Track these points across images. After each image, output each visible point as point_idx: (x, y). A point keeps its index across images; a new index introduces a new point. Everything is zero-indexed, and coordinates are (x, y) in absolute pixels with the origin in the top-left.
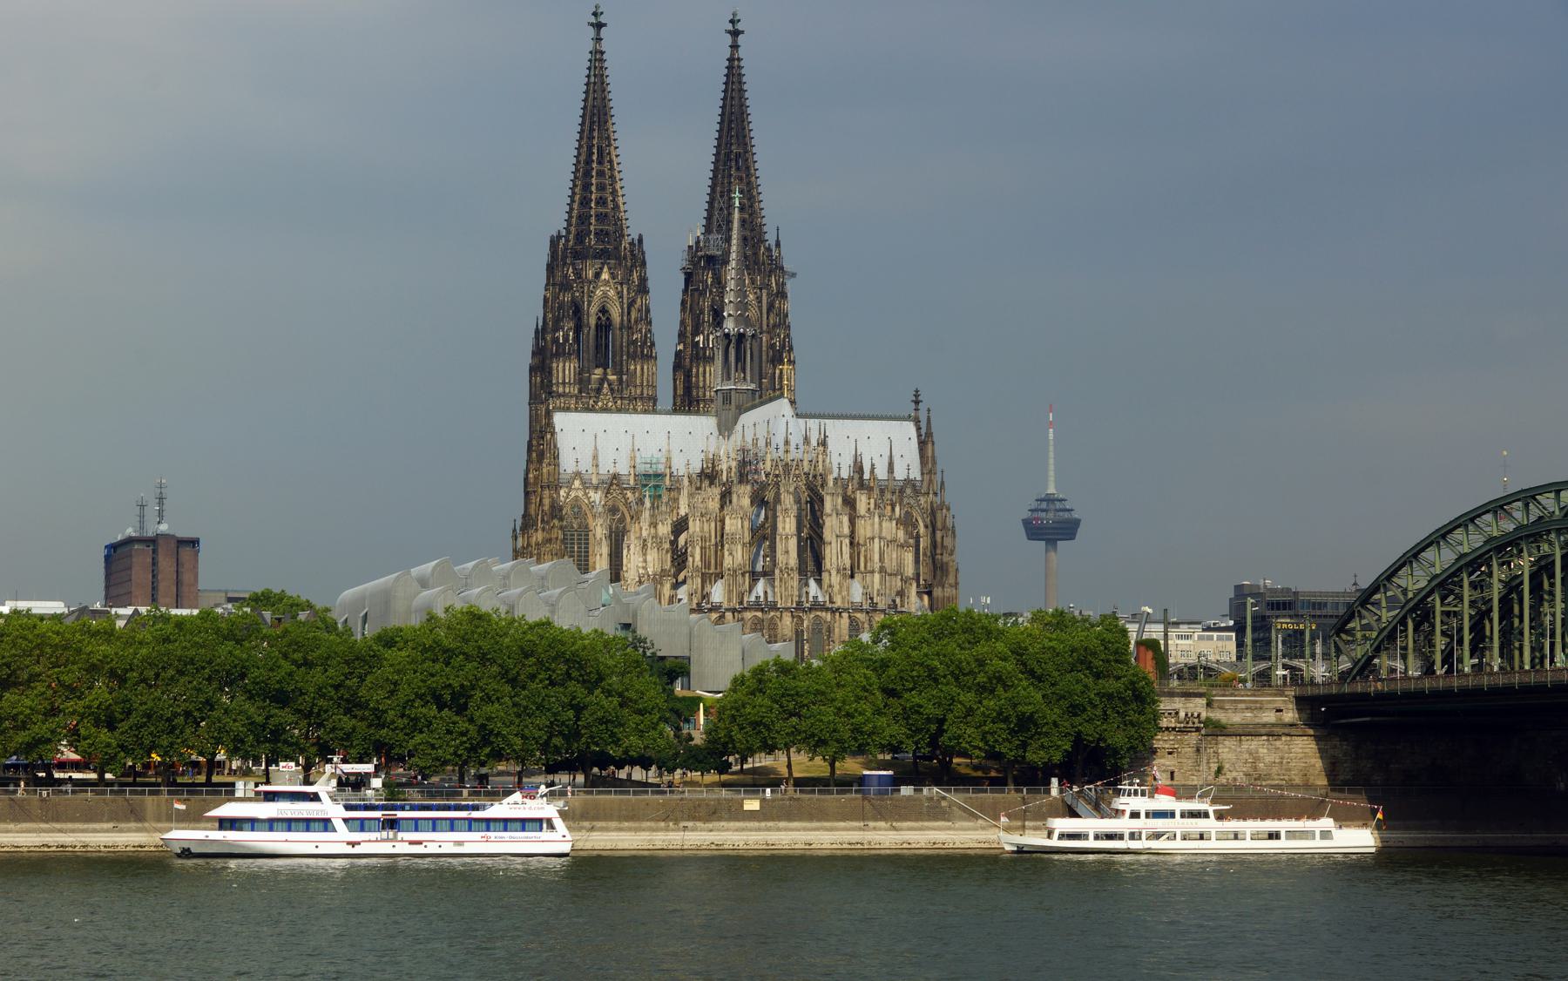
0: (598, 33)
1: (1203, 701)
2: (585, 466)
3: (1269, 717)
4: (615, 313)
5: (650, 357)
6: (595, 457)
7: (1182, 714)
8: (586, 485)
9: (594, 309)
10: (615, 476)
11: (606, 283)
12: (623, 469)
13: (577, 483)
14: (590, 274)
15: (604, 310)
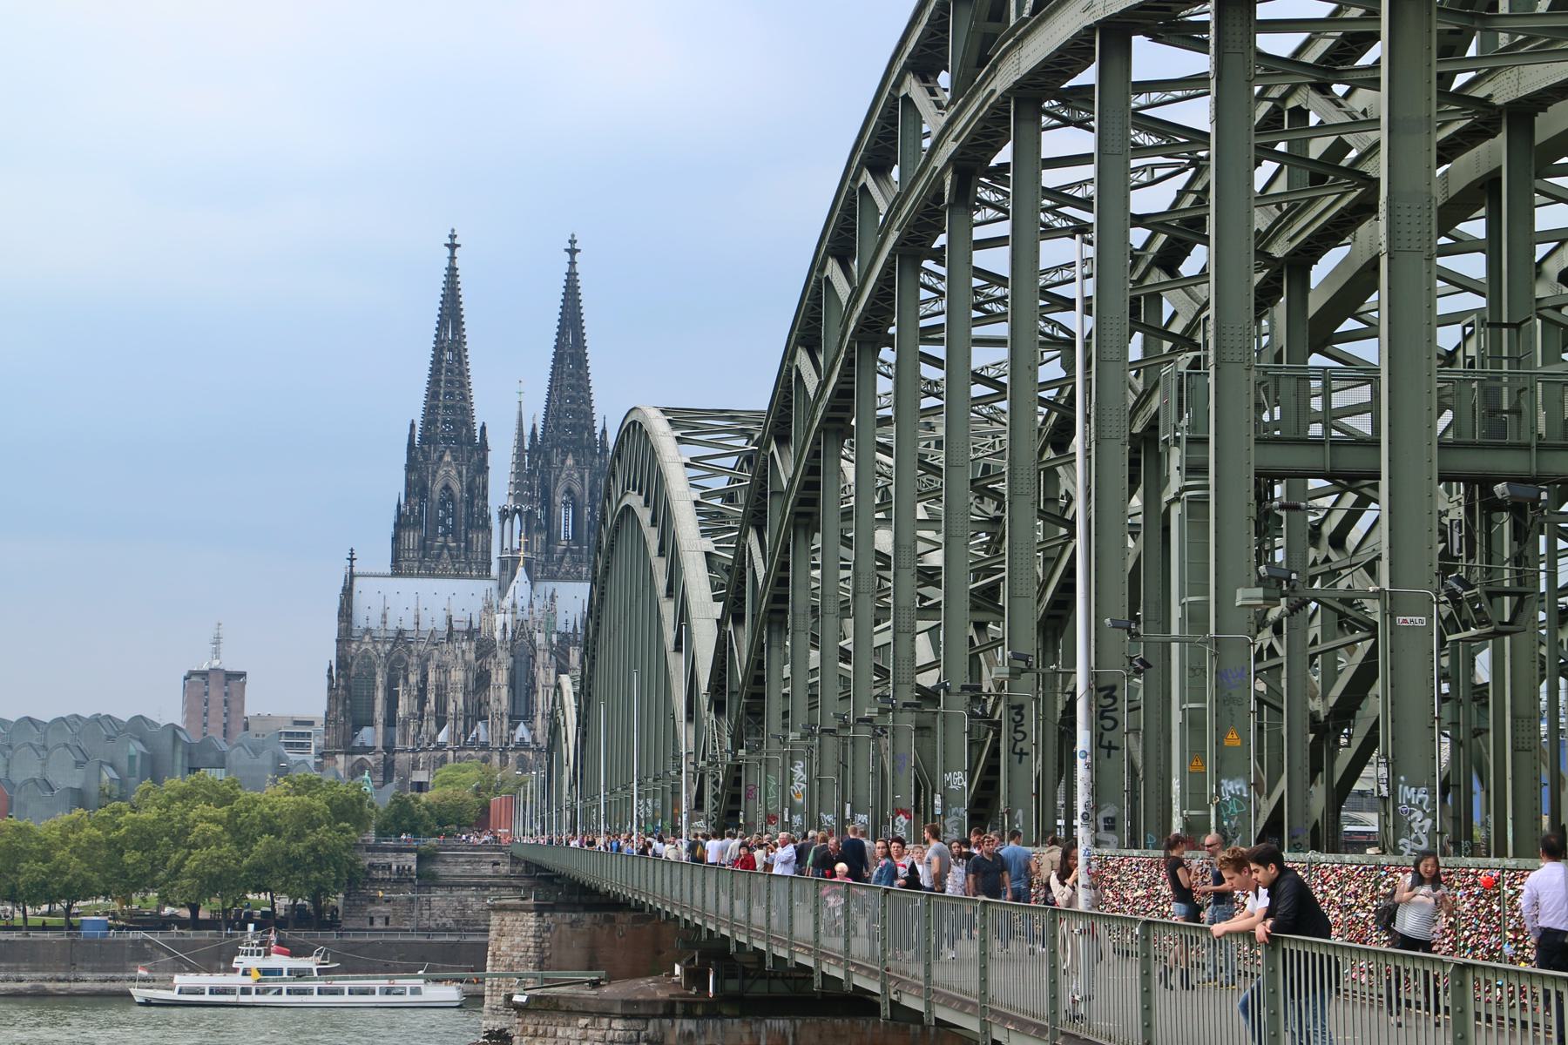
0: (453, 252)
1: (414, 856)
2: (375, 623)
3: (488, 870)
4: (456, 487)
5: (486, 528)
6: (384, 615)
7: (394, 867)
8: (374, 640)
9: (438, 487)
10: (401, 632)
11: (449, 464)
12: (408, 625)
13: (367, 638)
14: (435, 456)
15: (447, 488)
